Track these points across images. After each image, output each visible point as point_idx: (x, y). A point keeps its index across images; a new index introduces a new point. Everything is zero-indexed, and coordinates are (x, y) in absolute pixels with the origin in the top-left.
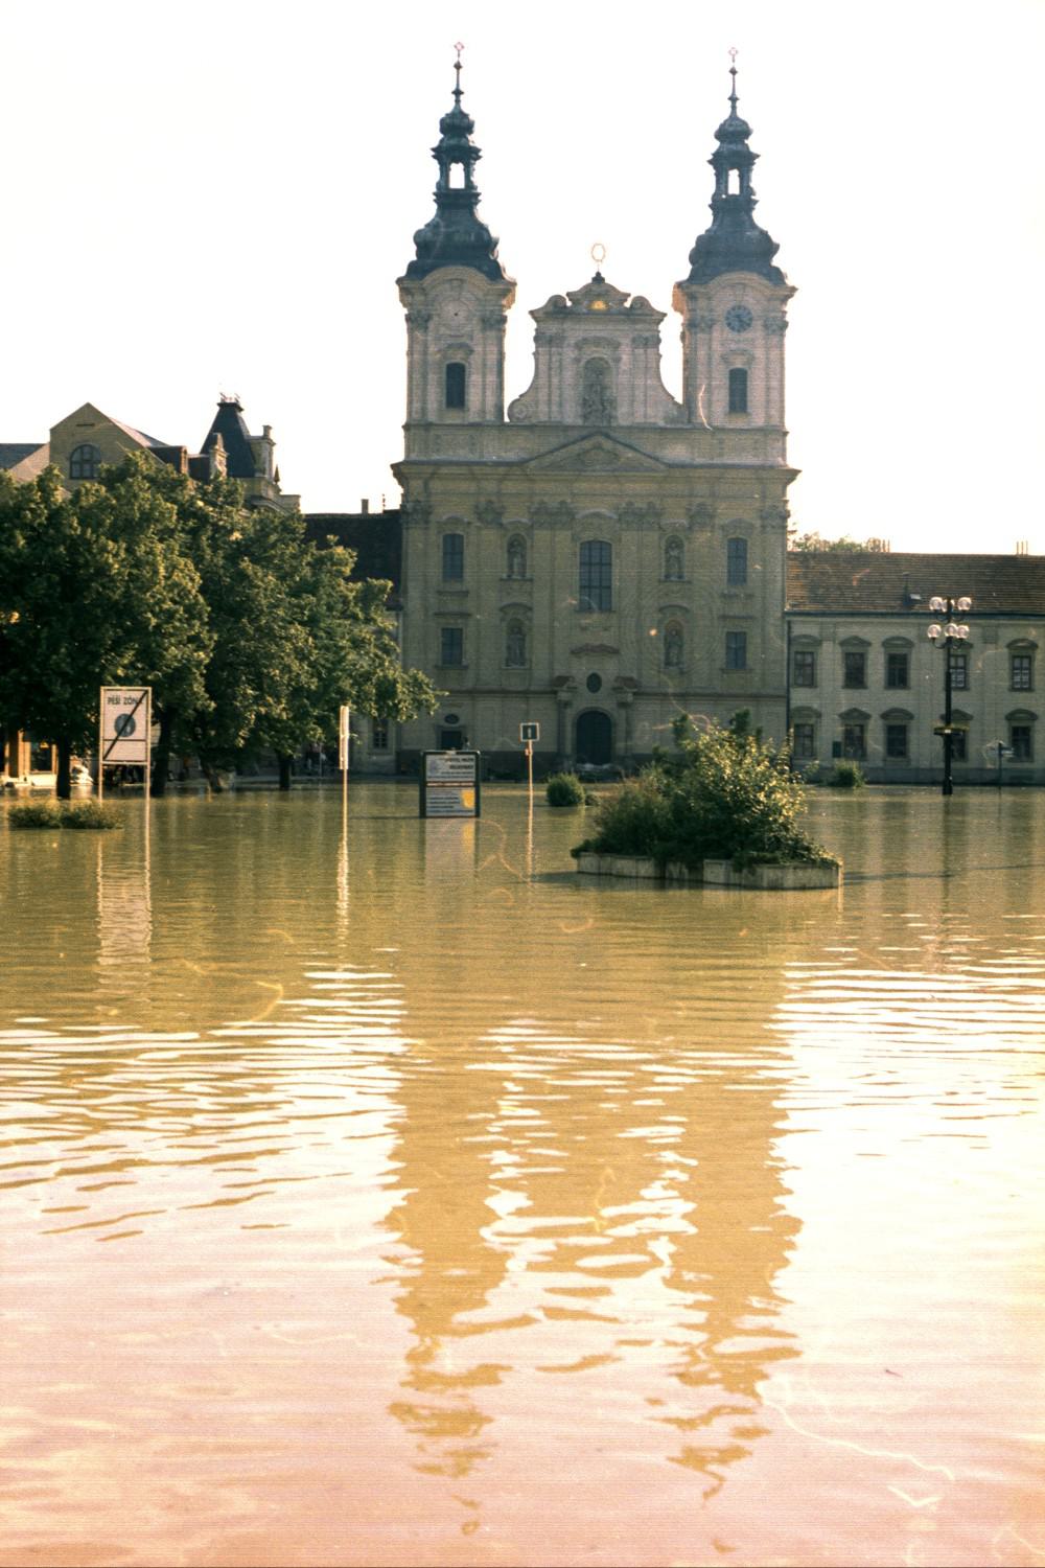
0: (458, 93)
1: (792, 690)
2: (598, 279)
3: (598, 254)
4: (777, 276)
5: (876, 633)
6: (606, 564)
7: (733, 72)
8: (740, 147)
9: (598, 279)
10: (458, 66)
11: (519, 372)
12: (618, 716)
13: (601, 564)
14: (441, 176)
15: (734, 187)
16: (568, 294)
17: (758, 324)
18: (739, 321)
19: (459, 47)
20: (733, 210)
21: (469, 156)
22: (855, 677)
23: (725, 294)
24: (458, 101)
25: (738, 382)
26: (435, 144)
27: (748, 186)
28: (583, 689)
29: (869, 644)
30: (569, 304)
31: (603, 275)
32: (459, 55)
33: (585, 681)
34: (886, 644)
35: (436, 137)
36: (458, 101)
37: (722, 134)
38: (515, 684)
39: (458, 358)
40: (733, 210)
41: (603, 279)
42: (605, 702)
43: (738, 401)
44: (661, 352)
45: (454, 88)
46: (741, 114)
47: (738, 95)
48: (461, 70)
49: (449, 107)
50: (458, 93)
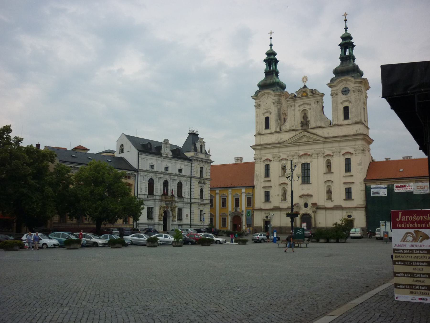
2: (305, 87)
3: (305, 80)
6: (303, 170)
8: (347, 41)
9: (305, 87)
10: (271, 38)
12: (312, 215)
13: (305, 170)
15: (347, 53)
17: (351, 91)
18: (345, 91)
19: (271, 33)
24: (271, 47)
25: (346, 109)
30: (297, 95)
31: (307, 86)
32: (271, 35)
33: (303, 205)
36: (271, 47)
39: (267, 115)
41: (307, 87)
42: (309, 211)
43: (346, 116)
45: (270, 44)
47: (347, 27)
48: (272, 39)
49: (268, 48)
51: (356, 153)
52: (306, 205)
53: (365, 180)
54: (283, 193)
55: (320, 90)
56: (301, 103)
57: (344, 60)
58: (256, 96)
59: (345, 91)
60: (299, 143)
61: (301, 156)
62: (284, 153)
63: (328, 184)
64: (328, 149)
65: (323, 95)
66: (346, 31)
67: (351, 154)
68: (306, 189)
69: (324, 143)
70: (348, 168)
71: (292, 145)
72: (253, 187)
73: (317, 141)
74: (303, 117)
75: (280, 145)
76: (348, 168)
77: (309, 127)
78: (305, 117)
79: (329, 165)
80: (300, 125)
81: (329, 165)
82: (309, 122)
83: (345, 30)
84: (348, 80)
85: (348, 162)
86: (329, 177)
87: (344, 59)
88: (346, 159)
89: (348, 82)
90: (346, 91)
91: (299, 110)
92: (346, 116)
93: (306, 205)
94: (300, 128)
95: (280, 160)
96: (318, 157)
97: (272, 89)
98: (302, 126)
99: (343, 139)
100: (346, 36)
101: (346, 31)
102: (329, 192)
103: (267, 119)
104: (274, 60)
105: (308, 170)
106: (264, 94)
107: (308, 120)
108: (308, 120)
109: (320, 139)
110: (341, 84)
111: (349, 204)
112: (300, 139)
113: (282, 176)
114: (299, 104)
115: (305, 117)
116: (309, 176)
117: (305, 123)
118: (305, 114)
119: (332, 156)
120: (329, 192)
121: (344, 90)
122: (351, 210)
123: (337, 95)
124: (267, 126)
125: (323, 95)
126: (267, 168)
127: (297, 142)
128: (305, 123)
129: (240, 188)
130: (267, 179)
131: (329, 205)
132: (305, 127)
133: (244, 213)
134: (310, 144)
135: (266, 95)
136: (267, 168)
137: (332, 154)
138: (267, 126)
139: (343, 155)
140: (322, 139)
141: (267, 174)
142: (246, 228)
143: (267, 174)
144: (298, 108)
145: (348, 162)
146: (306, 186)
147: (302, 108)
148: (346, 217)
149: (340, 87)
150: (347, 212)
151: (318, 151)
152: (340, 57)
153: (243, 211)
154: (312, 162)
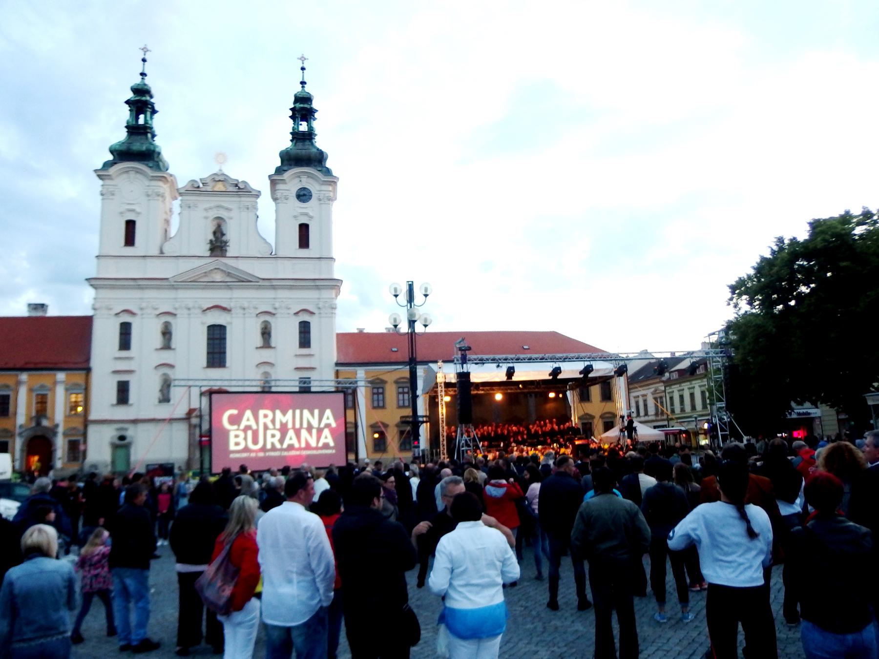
4: (328, 172)
7: (303, 69)
8: (306, 106)
16: (201, 180)
18: (303, 196)
20: (303, 138)
23: (295, 180)
25: (304, 229)
27: (311, 126)
30: (201, 185)
34: (396, 382)
37: (298, 99)
38: (164, 412)
40: (303, 138)
43: (304, 241)
44: (258, 213)
51: (320, 313)
53: (337, 364)
54: (162, 386)
55: (254, 185)
56: (212, 205)
58: (103, 172)
59: (303, 196)
60: (205, 284)
65: (258, 195)
66: (303, 87)
67: (312, 313)
69: (260, 287)
70: (305, 340)
71: (186, 286)
72: (88, 370)
73: (243, 281)
74: (215, 233)
76: (305, 340)
77: (228, 254)
79: (266, 333)
80: (208, 246)
81: (266, 333)
82: (228, 244)
83: (301, 85)
84: (310, 176)
85: (305, 329)
87: (298, 137)
88: (301, 323)
89: (310, 180)
90: (304, 195)
91: (206, 218)
92: (304, 241)
94: (208, 253)
96: (244, 314)
97: (146, 162)
100: (305, 96)
103: (130, 225)
104: (150, 106)
105: (223, 339)
107: (224, 238)
108: (224, 238)
109: (251, 280)
112: (205, 276)
113: (162, 349)
114: (207, 205)
116: (222, 353)
117: (218, 246)
118: (219, 226)
119: (274, 314)
121: (302, 193)
124: (130, 240)
125: (258, 195)
126: (125, 331)
127: (199, 280)
128: (218, 246)
129: (51, 372)
130: (124, 354)
132: (218, 252)
133: (61, 430)
134: (229, 288)
135: (132, 174)
136: (125, 331)
137: (273, 311)
138: (130, 240)
139: (296, 314)
140: (258, 280)
141: (125, 343)
142: (63, 463)
143: (125, 343)
144: (205, 214)
145: (305, 329)
146: (216, 373)
152: (291, 131)
153: (57, 426)
154: (231, 323)
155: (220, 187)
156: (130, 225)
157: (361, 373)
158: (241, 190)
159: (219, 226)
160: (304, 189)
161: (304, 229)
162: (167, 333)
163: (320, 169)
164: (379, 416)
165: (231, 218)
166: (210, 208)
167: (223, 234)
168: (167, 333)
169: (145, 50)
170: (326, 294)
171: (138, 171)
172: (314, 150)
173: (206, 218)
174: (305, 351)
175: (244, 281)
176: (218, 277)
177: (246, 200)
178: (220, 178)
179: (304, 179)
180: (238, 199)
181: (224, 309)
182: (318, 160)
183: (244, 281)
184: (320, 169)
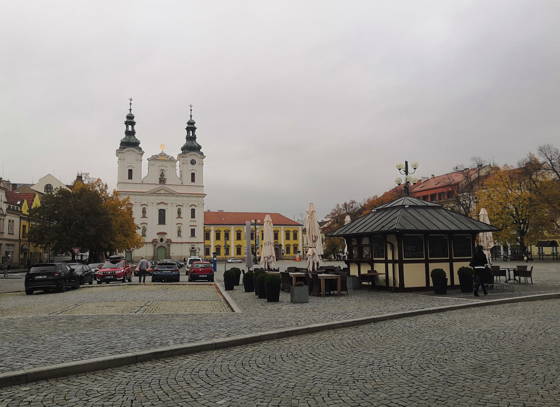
0: (130, 110)
1: (205, 241)
5: (222, 229)
7: (191, 110)
8: (193, 126)
10: (131, 104)
11: (145, 172)
14: (126, 128)
20: (191, 138)
21: (133, 124)
22: (218, 237)
25: (193, 175)
26: (126, 121)
28: (159, 242)
29: (221, 231)
34: (224, 231)
35: (126, 120)
36: (130, 112)
37: (189, 123)
40: (191, 138)
43: (193, 180)
46: (193, 119)
47: (192, 115)
50: (130, 110)
52: (162, 240)
57: (190, 139)
59: (193, 162)
61: (159, 203)
62: (144, 200)
63: (179, 225)
64: (179, 201)
67: (196, 206)
68: (162, 228)
70: (193, 216)
74: (161, 175)
75: (142, 194)
76: (193, 216)
78: (162, 175)
79: (179, 212)
80: (159, 181)
81: (179, 212)
84: (195, 155)
85: (193, 211)
86: (179, 221)
89: (195, 157)
91: (158, 170)
93: (162, 240)
95: (141, 205)
98: (160, 182)
99: (191, 195)
101: (191, 118)
102: (179, 232)
103: (130, 172)
106: (129, 151)
107: (164, 177)
110: (191, 156)
111: (193, 240)
113: (143, 217)
115: (162, 175)
117: (162, 180)
118: (163, 173)
120: (179, 232)
122: (194, 244)
123: (187, 164)
124: (130, 177)
128: (162, 180)
131: (179, 240)
132: (162, 183)
135: (131, 152)
138: (130, 177)
145: (193, 211)
147: (161, 168)
148: (191, 249)
149: (189, 159)
150: (191, 246)
151: (172, 202)
155: (163, 158)
156: (130, 172)
157: (212, 228)
158: (172, 160)
159: (163, 173)
160: (193, 160)
161: (193, 175)
162: (144, 211)
163: (199, 152)
164: (218, 243)
165: (167, 170)
166: (159, 166)
167: (164, 176)
168: (144, 211)
169: (131, 100)
170: (201, 199)
171: (133, 151)
172: (196, 145)
173: (158, 170)
174: (193, 219)
175: (172, 194)
176: (162, 192)
177: (173, 163)
178: (163, 155)
179: (193, 156)
180: (169, 163)
181: (165, 204)
182: (198, 148)
183: (172, 194)
184: (199, 152)
